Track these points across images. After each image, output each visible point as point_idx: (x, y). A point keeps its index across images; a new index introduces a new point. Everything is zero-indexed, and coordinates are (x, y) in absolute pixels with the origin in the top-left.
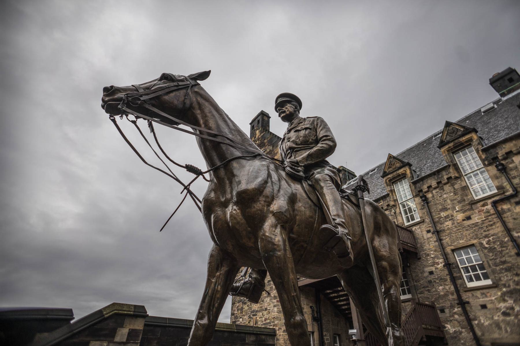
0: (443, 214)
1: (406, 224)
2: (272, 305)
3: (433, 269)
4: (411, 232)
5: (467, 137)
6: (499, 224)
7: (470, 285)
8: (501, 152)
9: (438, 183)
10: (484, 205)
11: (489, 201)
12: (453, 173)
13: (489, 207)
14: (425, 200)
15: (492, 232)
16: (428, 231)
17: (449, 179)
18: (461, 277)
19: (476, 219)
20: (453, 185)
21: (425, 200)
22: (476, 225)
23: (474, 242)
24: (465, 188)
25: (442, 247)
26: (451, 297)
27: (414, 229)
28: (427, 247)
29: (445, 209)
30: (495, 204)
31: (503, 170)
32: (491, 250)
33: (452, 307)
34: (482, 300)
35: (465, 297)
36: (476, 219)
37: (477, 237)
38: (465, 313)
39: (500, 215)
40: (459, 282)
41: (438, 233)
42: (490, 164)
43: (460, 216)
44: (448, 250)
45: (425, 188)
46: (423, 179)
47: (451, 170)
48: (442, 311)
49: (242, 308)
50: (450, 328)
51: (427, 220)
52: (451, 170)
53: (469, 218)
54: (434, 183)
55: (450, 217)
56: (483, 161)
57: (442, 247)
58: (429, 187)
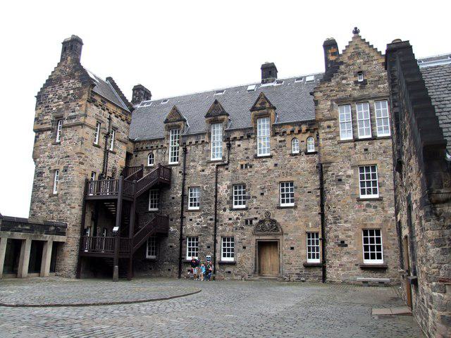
0: (192, 164)
1: (170, 163)
2: (66, 209)
3: (175, 196)
4: (170, 170)
5: (222, 117)
6: (215, 179)
7: (190, 208)
8: (232, 136)
9: (196, 142)
10: (213, 165)
11: (216, 164)
12: (206, 139)
13: (215, 167)
14: (185, 151)
15: (210, 182)
16: (180, 172)
17: (203, 141)
18: (187, 204)
19: (207, 172)
20: (203, 147)
21: (185, 151)
22: (205, 175)
23: (201, 185)
24: (209, 151)
25: (184, 184)
26: (178, 213)
27: (173, 168)
28: (176, 182)
29: (194, 161)
30: (218, 166)
31: (229, 147)
32: (206, 191)
33: (177, 219)
34: (191, 217)
35: (185, 214)
36: (207, 172)
37: (202, 183)
38: (182, 222)
39: (217, 172)
40: (185, 206)
41: (185, 174)
42: (225, 141)
43: (200, 168)
44: (186, 187)
45: (188, 143)
46: (189, 136)
47: (206, 137)
48: (172, 220)
49: (41, 207)
50: (172, 229)
51: (182, 165)
52: (206, 137)
53: (203, 171)
54: (194, 142)
55: (194, 167)
56: (224, 137)
57: (184, 184)
58: (191, 143)
